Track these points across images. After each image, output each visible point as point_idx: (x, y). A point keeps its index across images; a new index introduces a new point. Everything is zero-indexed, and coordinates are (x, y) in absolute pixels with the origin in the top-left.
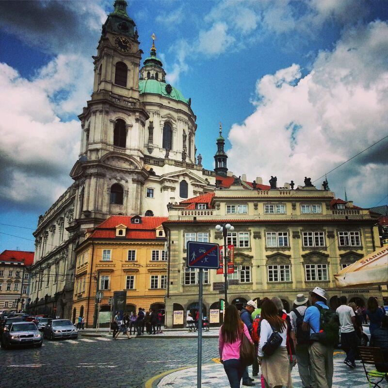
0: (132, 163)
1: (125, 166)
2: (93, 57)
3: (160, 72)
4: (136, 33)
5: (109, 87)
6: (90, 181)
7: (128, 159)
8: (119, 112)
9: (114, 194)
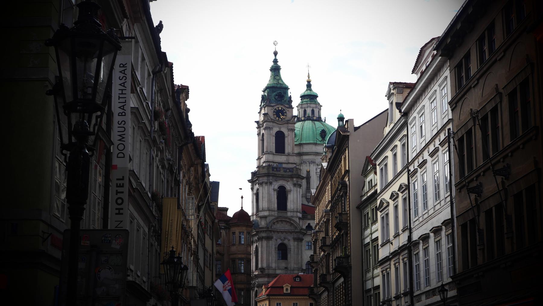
3: (316, 107)
4: (290, 97)
5: (271, 158)
7: (289, 221)
9: (280, 251)
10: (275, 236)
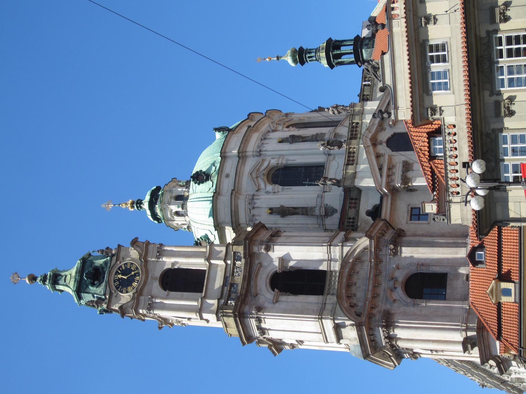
0: (358, 259)
1: (365, 270)
2: (160, 328)
3: (171, 191)
6: (400, 339)
8: (256, 286)
9: (426, 291)
10: (382, 306)
